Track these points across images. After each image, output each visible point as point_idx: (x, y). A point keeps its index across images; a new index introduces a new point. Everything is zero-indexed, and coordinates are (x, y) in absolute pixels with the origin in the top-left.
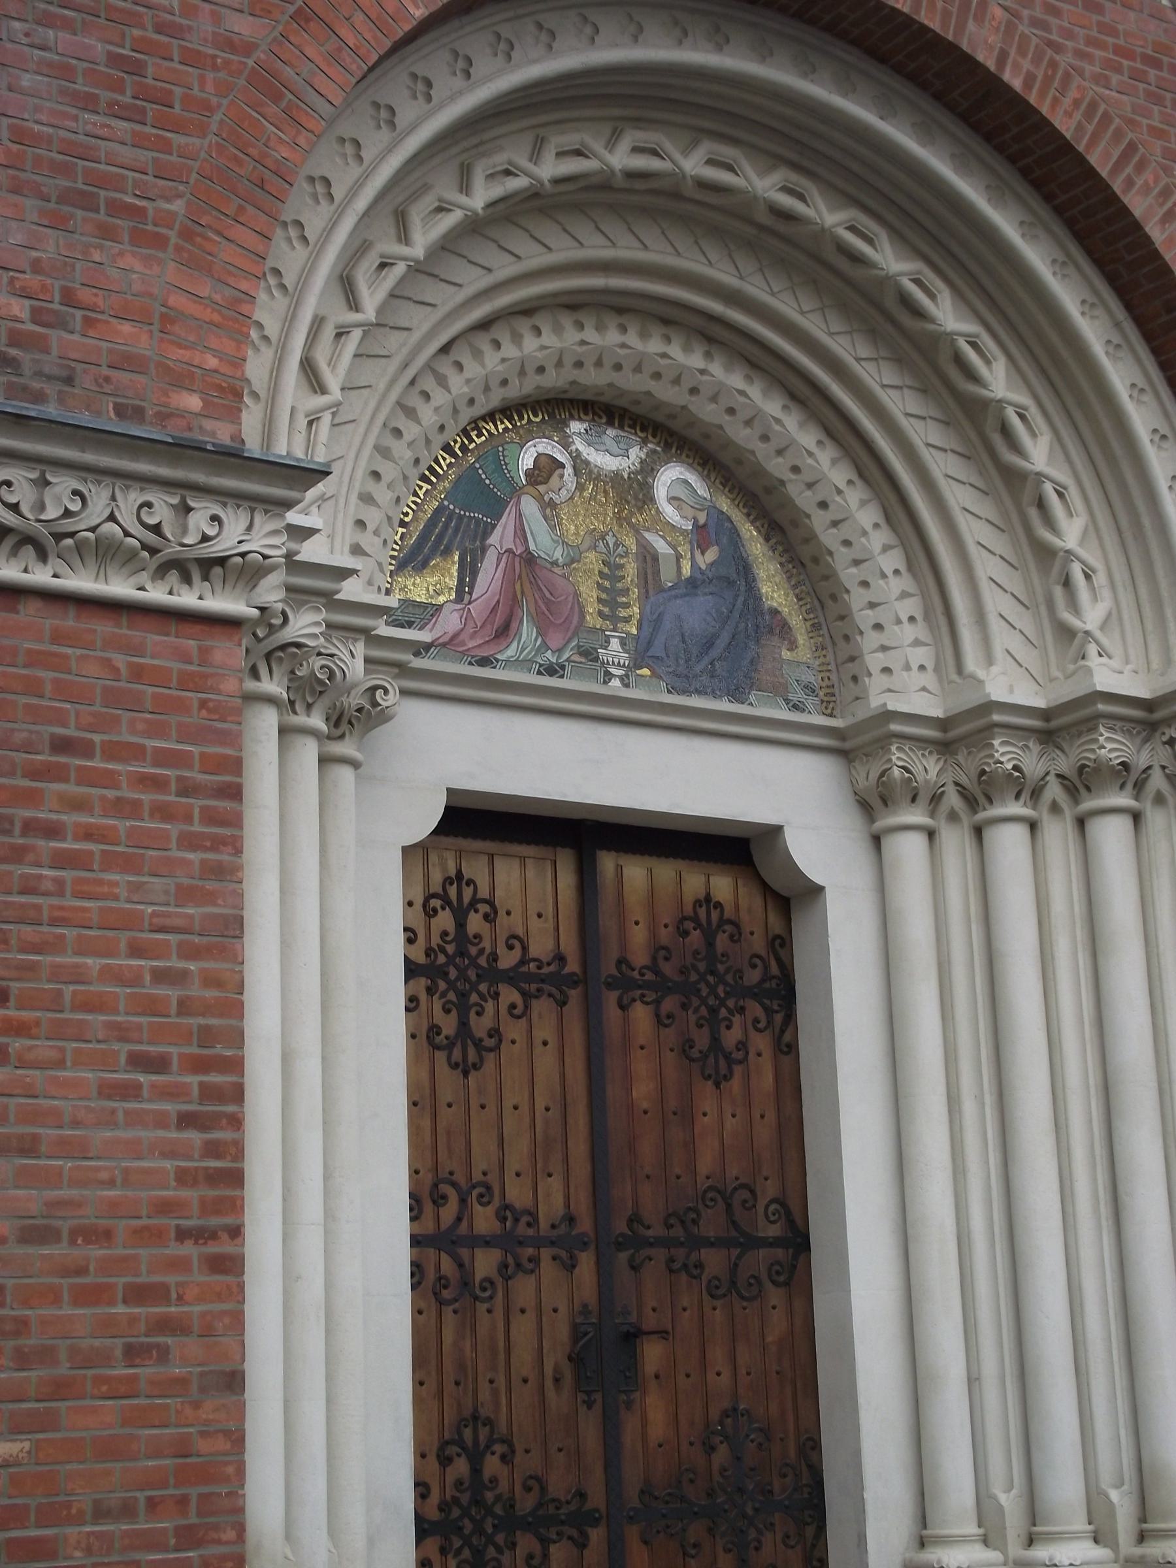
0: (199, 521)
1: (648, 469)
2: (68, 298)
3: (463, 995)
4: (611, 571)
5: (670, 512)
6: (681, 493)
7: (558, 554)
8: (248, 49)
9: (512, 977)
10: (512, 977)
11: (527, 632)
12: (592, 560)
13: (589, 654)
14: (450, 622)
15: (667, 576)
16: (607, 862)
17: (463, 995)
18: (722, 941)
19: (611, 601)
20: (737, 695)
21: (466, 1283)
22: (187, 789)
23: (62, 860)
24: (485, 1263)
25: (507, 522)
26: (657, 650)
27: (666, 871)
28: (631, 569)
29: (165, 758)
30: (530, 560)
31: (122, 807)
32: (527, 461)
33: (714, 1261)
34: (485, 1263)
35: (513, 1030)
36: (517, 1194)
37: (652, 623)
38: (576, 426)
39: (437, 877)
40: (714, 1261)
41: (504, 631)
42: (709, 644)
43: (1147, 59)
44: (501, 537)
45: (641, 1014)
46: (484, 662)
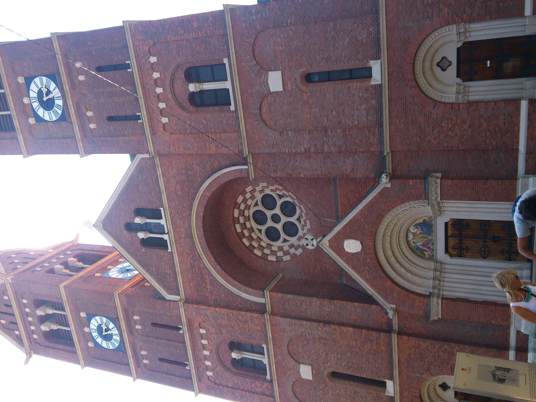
0: (435, 304)
1: (411, 233)
2: (420, 308)
3: (463, 249)
4: (422, 237)
5: (415, 231)
6: (413, 229)
7: (422, 242)
8: (397, 294)
9: (460, 244)
10: (460, 244)
11: (429, 246)
12: (421, 239)
13: (431, 240)
14: (429, 252)
15: (422, 232)
16: (449, 235)
17: (463, 249)
18: (456, 224)
19: (425, 238)
20: (432, 226)
21: (488, 251)
22: (454, 305)
23: (460, 313)
24: (487, 249)
25: (419, 246)
26: (429, 233)
27: (449, 229)
28: (421, 235)
29: (452, 306)
30: (422, 245)
31: (456, 309)
32: (413, 244)
33: (487, 228)
34: (487, 249)
35: (465, 244)
36: (481, 246)
37: (426, 234)
38: (409, 239)
39: (452, 250)
40: (487, 228)
41: (429, 248)
42: (427, 228)
43: (369, 211)
44: (421, 247)
45: (463, 233)
46: (433, 250)
